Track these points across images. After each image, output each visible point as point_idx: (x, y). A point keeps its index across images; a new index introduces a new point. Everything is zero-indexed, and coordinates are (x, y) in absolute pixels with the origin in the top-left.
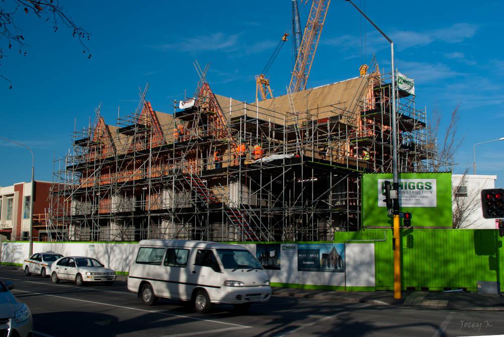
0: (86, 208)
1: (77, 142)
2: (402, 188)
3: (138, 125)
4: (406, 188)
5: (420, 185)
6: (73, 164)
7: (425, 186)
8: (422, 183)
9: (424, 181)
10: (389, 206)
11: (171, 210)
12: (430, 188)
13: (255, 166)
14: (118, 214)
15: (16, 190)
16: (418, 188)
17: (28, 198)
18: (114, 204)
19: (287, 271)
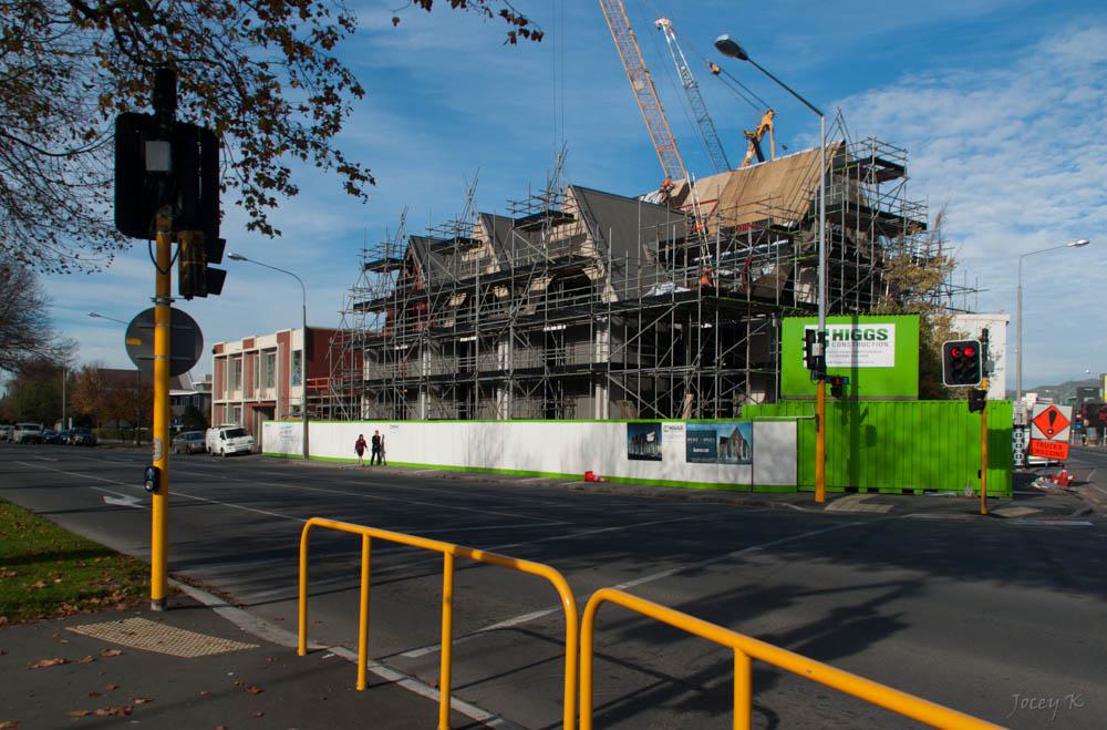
0: (385, 371)
1: (368, 267)
2: (841, 339)
3: (459, 238)
4: (847, 339)
5: (870, 333)
6: (363, 300)
7: (877, 335)
8: (872, 331)
9: (876, 327)
10: (810, 366)
11: (508, 371)
12: (886, 337)
13: (629, 304)
14: (433, 378)
15: (279, 341)
17: (298, 354)
18: (426, 365)
19: (674, 460)
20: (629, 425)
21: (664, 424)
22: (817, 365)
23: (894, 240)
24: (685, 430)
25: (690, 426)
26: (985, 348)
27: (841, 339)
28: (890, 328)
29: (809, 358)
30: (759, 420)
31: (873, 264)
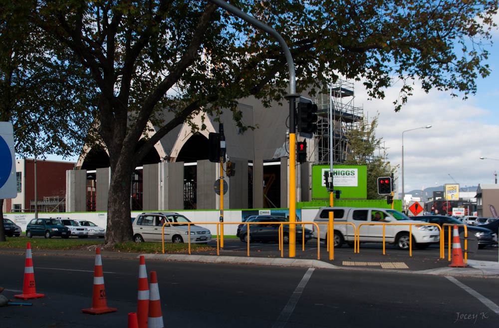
2: (337, 175)
4: (339, 175)
8: (349, 171)
9: (350, 170)
10: (327, 186)
12: (354, 174)
16: (346, 174)
20: (243, 212)
21: (260, 211)
22: (330, 186)
23: (348, 124)
24: (270, 212)
25: (272, 211)
26: (393, 181)
27: (337, 175)
28: (356, 170)
29: (327, 183)
30: (304, 209)
31: (341, 137)
